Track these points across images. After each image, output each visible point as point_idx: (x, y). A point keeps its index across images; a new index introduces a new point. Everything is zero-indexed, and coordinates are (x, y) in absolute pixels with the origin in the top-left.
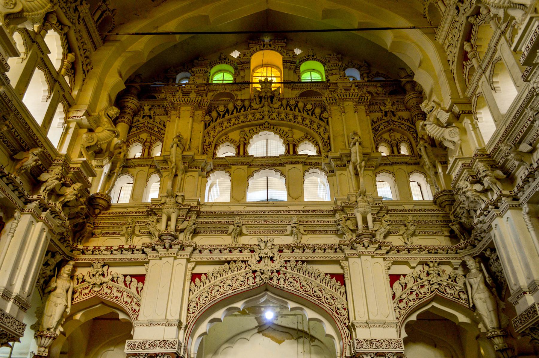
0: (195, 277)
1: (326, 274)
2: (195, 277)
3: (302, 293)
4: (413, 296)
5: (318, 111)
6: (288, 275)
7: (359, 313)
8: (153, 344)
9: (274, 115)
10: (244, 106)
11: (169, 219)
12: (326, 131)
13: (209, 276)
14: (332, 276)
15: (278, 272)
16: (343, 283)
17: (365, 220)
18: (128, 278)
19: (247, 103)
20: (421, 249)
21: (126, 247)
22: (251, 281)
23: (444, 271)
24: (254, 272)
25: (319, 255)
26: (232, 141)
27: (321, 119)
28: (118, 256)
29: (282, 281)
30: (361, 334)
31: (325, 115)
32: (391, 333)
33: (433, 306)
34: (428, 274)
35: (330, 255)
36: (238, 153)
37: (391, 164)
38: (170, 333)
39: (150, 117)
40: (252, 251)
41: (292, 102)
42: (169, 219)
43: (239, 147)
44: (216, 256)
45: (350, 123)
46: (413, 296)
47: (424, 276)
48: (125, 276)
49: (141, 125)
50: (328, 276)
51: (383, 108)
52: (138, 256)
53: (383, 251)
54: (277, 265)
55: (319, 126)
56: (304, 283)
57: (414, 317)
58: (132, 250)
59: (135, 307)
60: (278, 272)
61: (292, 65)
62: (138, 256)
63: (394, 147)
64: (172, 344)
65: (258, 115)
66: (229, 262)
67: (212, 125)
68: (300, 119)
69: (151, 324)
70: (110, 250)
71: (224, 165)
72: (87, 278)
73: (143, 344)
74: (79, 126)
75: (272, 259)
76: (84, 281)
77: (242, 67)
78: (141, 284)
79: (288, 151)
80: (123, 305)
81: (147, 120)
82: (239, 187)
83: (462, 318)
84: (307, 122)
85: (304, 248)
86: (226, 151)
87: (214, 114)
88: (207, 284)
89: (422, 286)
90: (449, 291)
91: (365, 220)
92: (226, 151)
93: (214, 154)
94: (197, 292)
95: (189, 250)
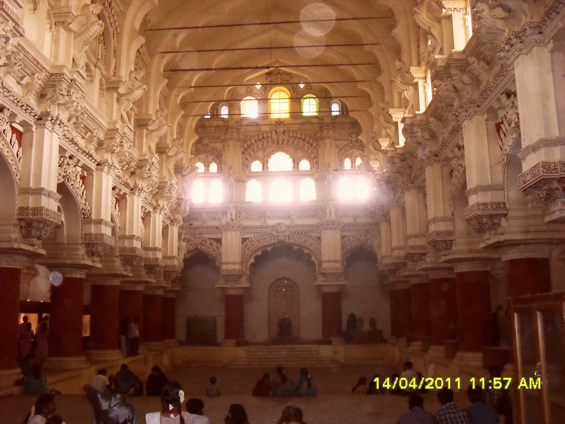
11: (231, 214)
36: (263, 169)
42: (231, 214)
61: (296, 99)
71: (256, 175)
92: (256, 166)
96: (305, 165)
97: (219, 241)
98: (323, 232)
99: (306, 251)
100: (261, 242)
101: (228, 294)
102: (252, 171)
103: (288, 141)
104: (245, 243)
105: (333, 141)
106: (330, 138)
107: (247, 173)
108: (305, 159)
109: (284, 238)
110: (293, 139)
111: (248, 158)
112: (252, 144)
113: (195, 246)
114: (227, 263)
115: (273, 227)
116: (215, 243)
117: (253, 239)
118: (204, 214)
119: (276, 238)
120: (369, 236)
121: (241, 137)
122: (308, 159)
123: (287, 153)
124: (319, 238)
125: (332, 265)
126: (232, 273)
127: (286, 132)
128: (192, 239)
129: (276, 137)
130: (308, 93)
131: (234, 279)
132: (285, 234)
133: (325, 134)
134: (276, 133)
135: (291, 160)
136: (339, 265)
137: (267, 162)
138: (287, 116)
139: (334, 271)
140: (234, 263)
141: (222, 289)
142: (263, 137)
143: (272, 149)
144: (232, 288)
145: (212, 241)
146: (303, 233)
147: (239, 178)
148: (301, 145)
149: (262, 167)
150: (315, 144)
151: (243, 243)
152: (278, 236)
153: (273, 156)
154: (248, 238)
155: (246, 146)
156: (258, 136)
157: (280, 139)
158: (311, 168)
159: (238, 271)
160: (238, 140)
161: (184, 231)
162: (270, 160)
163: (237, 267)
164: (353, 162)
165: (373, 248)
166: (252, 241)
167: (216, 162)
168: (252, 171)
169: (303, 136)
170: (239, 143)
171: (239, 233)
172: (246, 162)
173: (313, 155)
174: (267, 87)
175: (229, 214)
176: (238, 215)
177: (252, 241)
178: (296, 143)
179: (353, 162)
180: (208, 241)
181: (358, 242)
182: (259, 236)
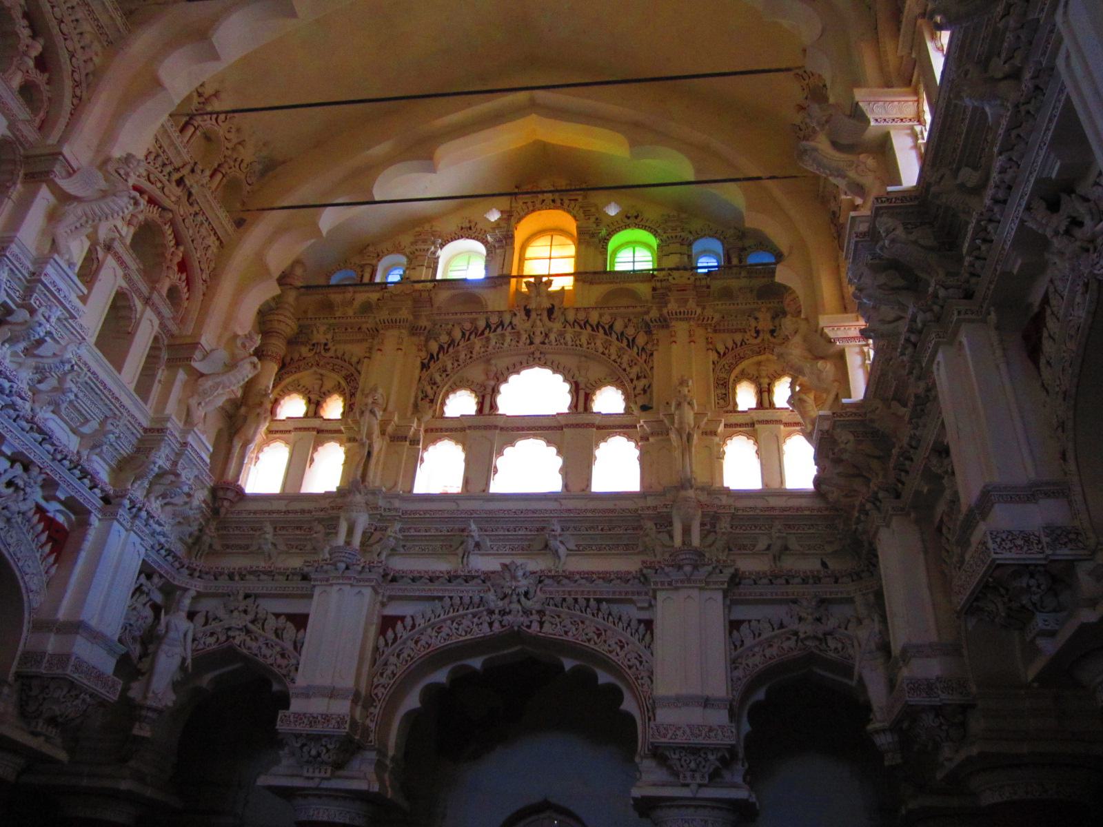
11: (350, 532)
36: (480, 410)
42: (350, 532)
71: (458, 430)
77: (501, 245)
82: (479, 468)
86: (461, 404)
91: (687, 531)
92: (461, 404)
96: (609, 401)
97: (300, 621)
98: (661, 596)
99: (604, 678)
100: (445, 630)
103: (562, 334)
104: (390, 634)
105: (700, 333)
106: (686, 317)
107: (428, 417)
108: (611, 384)
109: (526, 621)
110: (577, 328)
111: (438, 379)
112: (452, 343)
113: (223, 638)
114: (307, 693)
115: (486, 577)
116: (290, 630)
117: (419, 621)
118: (269, 528)
119: (496, 617)
120: (831, 623)
121: (424, 322)
122: (619, 384)
123: (556, 370)
124: (649, 624)
125: (695, 716)
126: (318, 729)
127: (556, 313)
128: (221, 613)
129: (528, 325)
130: (627, 227)
131: (324, 757)
132: (528, 604)
133: (672, 306)
134: (528, 313)
135: (567, 387)
136: (720, 717)
137: (495, 391)
139: (700, 740)
140: (332, 693)
142: (488, 326)
143: (515, 359)
145: (282, 619)
146: (592, 603)
148: (599, 343)
150: (641, 340)
151: (382, 631)
152: (503, 613)
153: (513, 379)
154: (402, 618)
155: (434, 347)
156: (473, 321)
157: (539, 329)
158: (627, 408)
159: (341, 721)
160: (414, 331)
161: (197, 586)
162: (504, 388)
163: (342, 707)
164: (764, 394)
165: (847, 670)
166: (413, 626)
167: (342, 393)
169: (606, 319)
170: (415, 339)
171: (368, 592)
172: (428, 389)
173: (635, 371)
175: (343, 528)
176: (377, 535)
177: (413, 626)
178: (584, 340)
179: (764, 394)
180: (272, 623)
181: (792, 643)
182: (439, 611)
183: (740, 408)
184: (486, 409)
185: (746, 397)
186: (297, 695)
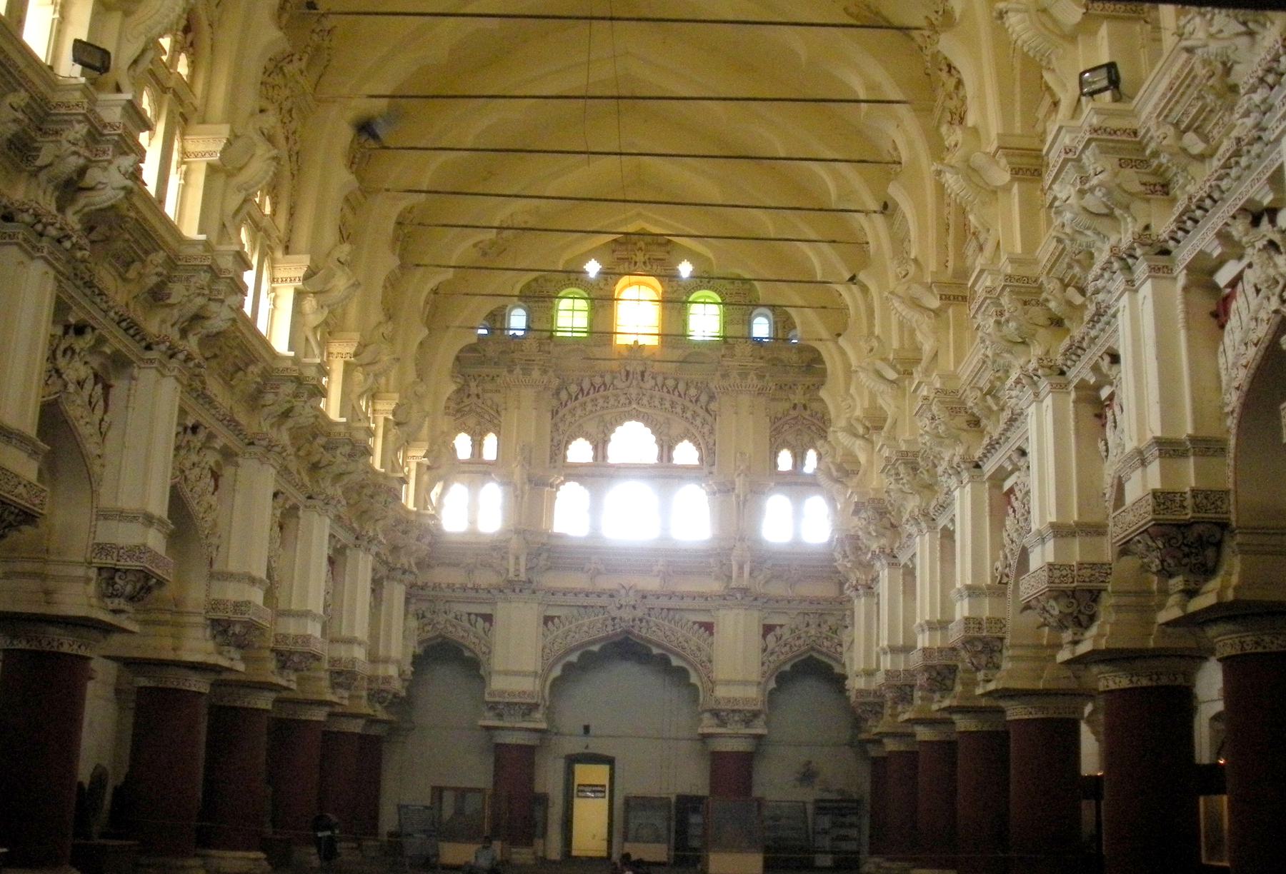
0: (548, 620)
1: (694, 623)
2: (548, 620)
3: (666, 643)
4: (787, 648)
5: (704, 398)
6: (652, 624)
7: (722, 670)
8: (512, 694)
9: (645, 401)
10: (604, 384)
11: (517, 558)
12: (712, 432)
13: (563, 618)
14: (702, 625)
15: (641, 620)
16: (712, 634)
17: (741, 568)
18: (473, 617)
19: (608, 379)
20: (803, 600)
21: (470, 585)
22: (610, 628)
23: (826, 622)
24: (614, 619)
25: (687, 603)
26: (587, 436)
27: (707, 410)
28: (459, 594)
29: (644, 631)
30: (721, 692)
31: (713, 406)
32: (752, 692)
33: (811, 656)
34: (808, 625)
35: (699, 603)
36: (595, 458)
37: (789, 484)
38: (528, 685)
39: (478, 396)
40: (612, 596)
41: (670, 383)
42: (517, 558)
43: (595, 448)
44: (570, 599)
45: (742, 421)
46: (787, 648)
47: (802, 627)
48: (469, 614)
49: (467, 409)
50: (696, 626)
51: (792, 397)
52: (484, 595)
53: (758, 603)
54: (639, 613)
55: (704, 422)
56: (668, 633)
57: (787, 668)
58: (476, 589)
59: (484, 649)
60: (641, 620)
61: (675, 303)
62: (484, 595)
63: (799, 458)
64: (531, 695)
65: (623, 400)
66: (585, 607)
67: (560, 414)
68: (679, 410)
69: (506, 673)
70: (451, 587)
72: (428, 615)
73: (502, 693)
74: (418, 464)
75: (634, 607)
76: (423, 617)
78: (487, 624)
79: (661, 458)
80: (472, 646)
81: (474, 399)
82: (595, 509)
83: (837, 669)
84: (689, 414)
85: (671, 596)
87: (564, 395)
88: (561, 630)
89: (799, 638)
90: (826, 643)
91: (741, 568)
92: (579, 451)
93: (565, 457)
94: (550, 637)
95: (540, 595)
96: (686, 453)
101: (500, 741)
102: (569, 460)
137: (605, 442)
138: (654, 341)
141: (488, 728)
144: (513, 729)
147: (536, 476)
149: (592, 454)
168: (569, 460)
174: (610, 275)
183: (780, 469)
184: (600, 459)
185: (785, 460)
186: (499, 673)
